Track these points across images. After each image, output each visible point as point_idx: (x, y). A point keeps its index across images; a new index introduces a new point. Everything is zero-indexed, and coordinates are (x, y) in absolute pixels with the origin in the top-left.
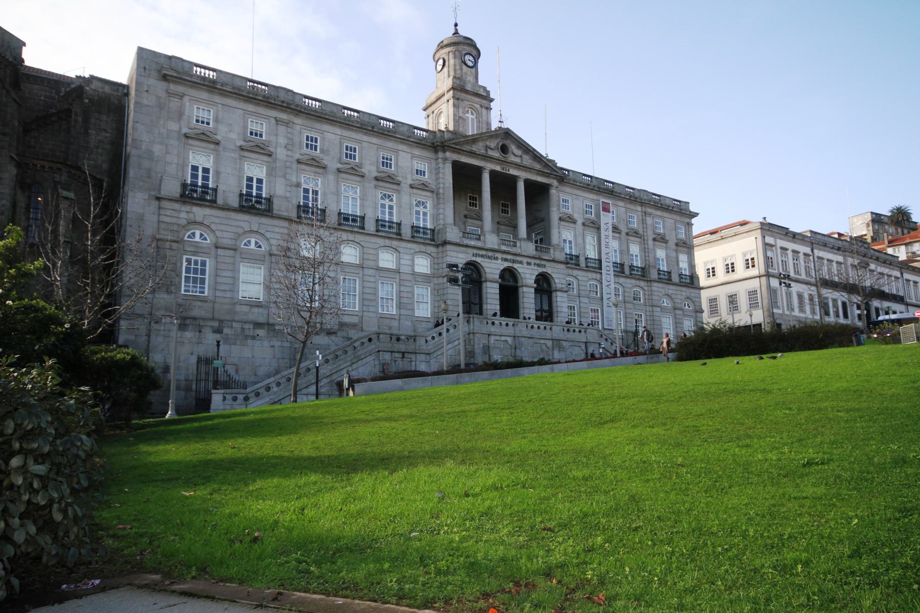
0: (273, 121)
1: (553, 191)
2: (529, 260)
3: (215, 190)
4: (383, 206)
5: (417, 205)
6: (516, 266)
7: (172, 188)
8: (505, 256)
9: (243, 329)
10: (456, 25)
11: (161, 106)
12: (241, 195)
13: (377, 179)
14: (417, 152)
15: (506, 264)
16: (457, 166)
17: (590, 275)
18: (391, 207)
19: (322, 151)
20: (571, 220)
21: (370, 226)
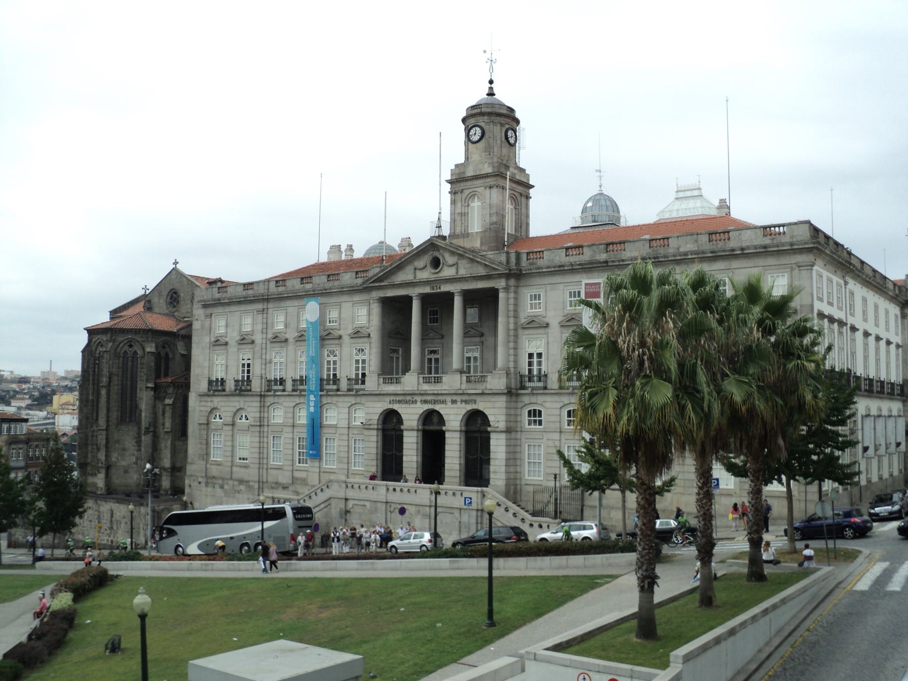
0: (255, 312)
1: (502, 295)
2: (454, 398)
5: (357, 355)
6: (437, 407)
7: (204, 386)
8: (424, 398)
9: (234, 485)
10: (491, 82)
11: (203, 327)
14: (357, 298)
17: (566, 399)
18: (335, 363)
19: (286, 326)
20: (537, 325)
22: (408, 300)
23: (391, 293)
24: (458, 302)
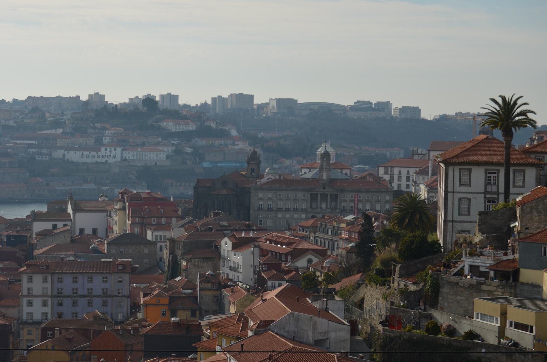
1: (339, 195)
3: (263, 208)
4: (295, 205)
7: (256, 209)
12: (267, 208)
13: (294, 200)
15: (323, 215)
16: (311, 195)
18: (297, 205)
20: (345, 201)
21: (292, 210)
22: (317, 194)
23: (313, 193)
24: (329, 196)
